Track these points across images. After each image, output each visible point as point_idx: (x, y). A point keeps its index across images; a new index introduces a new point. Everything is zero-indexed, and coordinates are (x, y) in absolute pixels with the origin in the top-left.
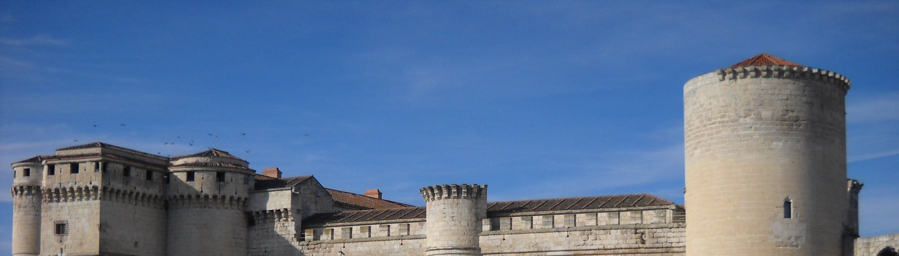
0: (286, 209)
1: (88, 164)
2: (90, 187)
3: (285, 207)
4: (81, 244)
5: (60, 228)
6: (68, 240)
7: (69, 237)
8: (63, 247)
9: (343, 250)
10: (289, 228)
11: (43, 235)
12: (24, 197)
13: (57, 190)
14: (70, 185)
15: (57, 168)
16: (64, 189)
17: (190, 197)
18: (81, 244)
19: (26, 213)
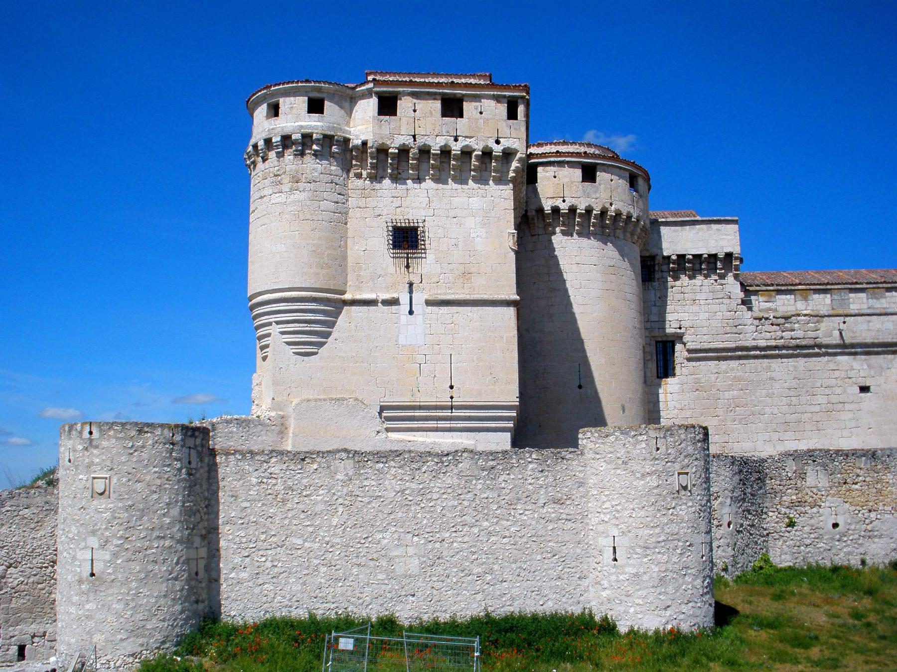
0: (729, 255)
1: (488, 105)
2: (497, 149)
3: (728, 250)
4: (466, 275)
5: (406, 239)
6: (428, 264)
7: (430, 256)
8: (416, 280)
9: (842, 326)
10: (728, 288)
11: (354, 250)
12: (309, 159)
13: (404, 151)
14: (440, 142)
15: (404, 105)
16: (425, 151)
17: (589, 211)
18: (466, 275)
19: (316, 197)
